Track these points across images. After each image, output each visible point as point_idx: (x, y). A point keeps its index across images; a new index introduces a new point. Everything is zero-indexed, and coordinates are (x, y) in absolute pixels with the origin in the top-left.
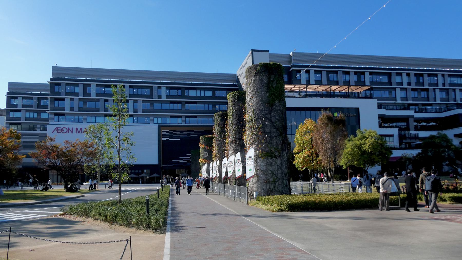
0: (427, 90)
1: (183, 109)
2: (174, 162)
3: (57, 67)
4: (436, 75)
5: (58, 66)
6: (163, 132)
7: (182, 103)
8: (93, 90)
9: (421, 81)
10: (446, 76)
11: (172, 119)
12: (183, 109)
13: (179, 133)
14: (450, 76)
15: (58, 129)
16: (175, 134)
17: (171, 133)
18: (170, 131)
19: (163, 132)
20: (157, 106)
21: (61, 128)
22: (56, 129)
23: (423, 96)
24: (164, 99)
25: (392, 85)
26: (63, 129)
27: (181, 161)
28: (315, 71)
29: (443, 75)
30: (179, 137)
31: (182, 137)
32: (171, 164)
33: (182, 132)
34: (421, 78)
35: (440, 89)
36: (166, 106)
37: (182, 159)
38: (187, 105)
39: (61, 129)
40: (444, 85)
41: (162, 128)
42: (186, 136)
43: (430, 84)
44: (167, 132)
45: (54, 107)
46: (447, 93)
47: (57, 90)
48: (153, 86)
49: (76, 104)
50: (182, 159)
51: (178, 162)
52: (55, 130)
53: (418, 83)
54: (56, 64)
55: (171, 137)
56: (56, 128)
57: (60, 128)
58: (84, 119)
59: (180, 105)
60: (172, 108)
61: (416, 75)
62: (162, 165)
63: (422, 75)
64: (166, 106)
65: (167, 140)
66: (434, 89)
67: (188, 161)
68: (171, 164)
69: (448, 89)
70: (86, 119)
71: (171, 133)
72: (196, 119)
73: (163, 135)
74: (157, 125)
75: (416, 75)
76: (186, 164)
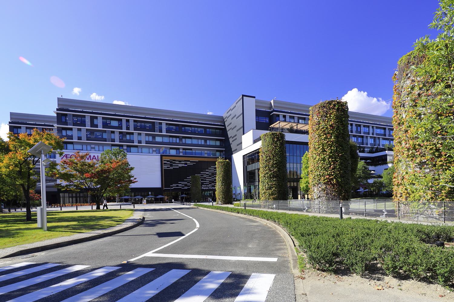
0: (362, 137)
1: (181, 142)
2: (174, 186)
3: (62, 98)
4: (368, 127)
5: (63, 97)
6: (164, 161)
7: (180, 137)
8: (99, 122)
9: (359, 130)
10: (375, 128)
11: (171, 150)
12: (181, 142)
13: (178, 162)
14: (377, 128)
15: (67, 156)
16: (175, 163)
17: (171, 162)
18: (170, 160)
19: (164, 161)
20: (158, 139)
21: (70, 155)
22: (66, 156)
23: (359, 141)
24: (164, 133)
25: (352, 133)
26: (72, 156)
27: (179, 185)
28: (290, 116)
29: (373, 127)
30: (178, 165)
31: (180, 165)
32: (172, 187)
33: (180, 161)
34: (359, 127)
35: (370, 137)
36: (166, 140)
37: (181, 183)
38: (183, 140)
39: (70, 156)
40: (373, 134)
41: (163, 157)
42: (184, 165)
43: (364, 133)
44: (168, 161)
45: (62, 135)
46: (375, 141)
47: (64, 120)
48: (154, 122)
49: (84, 134)
50: (181, 183)
51: (178, 186)
52: (64, 157)
53: (357, 131)
54: (62, 96)
55: (171, 165)
56: (65, 155)
57: (69, 155)
58: (92, 148)
59: (178, 139)
60: (171, 141)
61: (356, 125)
62: (164, 188)
63: (360, 126)
64: (166, 140)
65: (168, 167)
66: (367, 136)
67: (186, 185)
68: (172, 187)
69: (375, 137)
70: (94, 148)
71: (171, 162)
72: (191, 151)
73: (165, 164)
74: (160, 155)
75: (356, 125)
76: (184, 187)
